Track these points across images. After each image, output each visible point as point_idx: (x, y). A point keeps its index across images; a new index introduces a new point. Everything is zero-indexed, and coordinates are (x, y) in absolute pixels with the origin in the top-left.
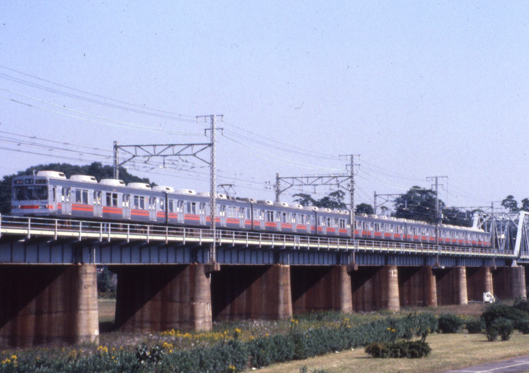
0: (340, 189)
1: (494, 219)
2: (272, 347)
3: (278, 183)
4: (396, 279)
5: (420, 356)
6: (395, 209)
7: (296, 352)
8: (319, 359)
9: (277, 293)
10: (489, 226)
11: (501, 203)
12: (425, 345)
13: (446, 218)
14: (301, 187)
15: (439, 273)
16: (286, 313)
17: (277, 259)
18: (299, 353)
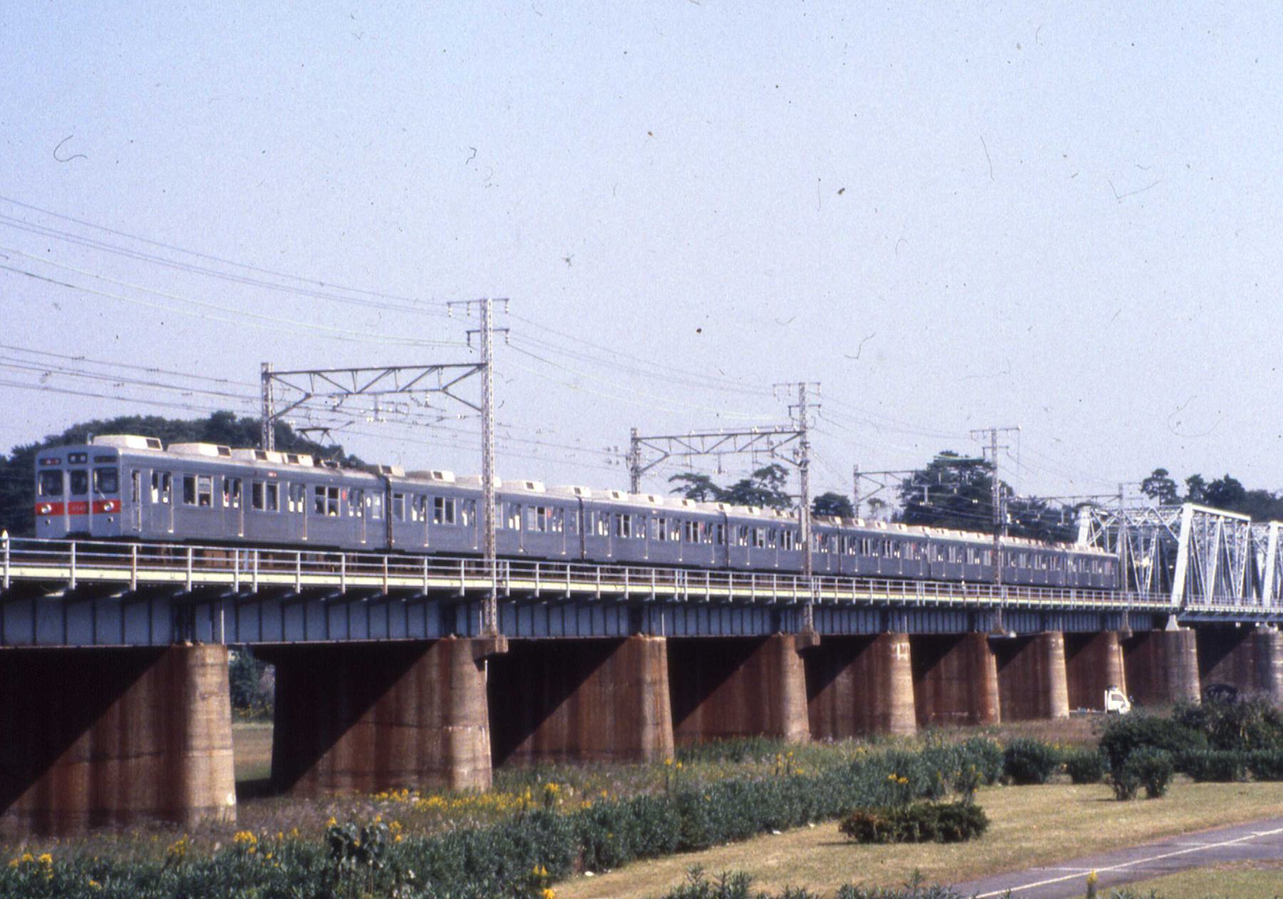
0: (778, 461)
1: (1125, 524)
2: (628, 824)
3: (635, 450)
4: (908, 665)
5: (965, 836)
6: (901, 506)
7: (684, 834)
8: (735, 849)
9: (639, 702)
10: (1113, 539)
11: (1140, 487)
12: (976, 811)
13: (1018, 522)
14: (688, 458)
15: (1005, 650)
16: (659, 749)
17: (636, 625)
18: (691, 836)
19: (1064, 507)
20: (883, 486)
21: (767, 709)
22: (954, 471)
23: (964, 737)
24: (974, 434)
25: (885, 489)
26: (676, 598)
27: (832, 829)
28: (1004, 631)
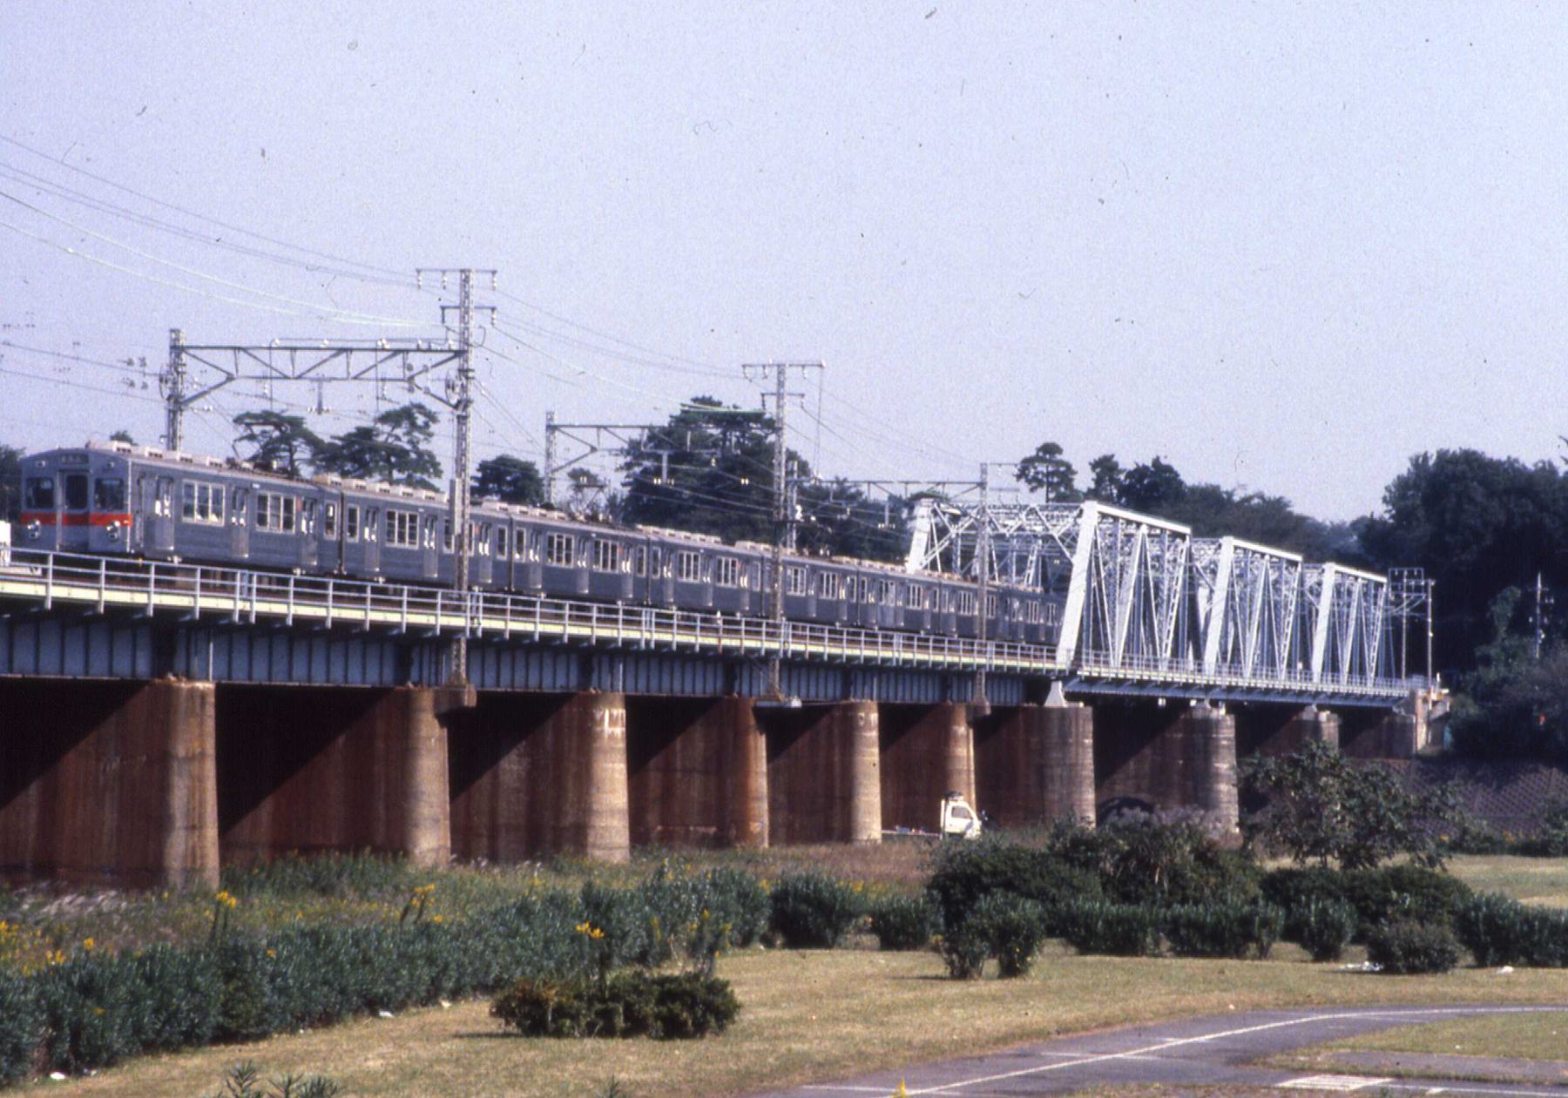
0: (419, 397)
1: (988, 530)
2: (132, 993)
3: (176, 367)
4: (621, 745)
5: (699, 1030)
6: (624, 485)
7: (226, 1014)
8: (315, 1040)
9: (164, 788)
10: (968, 555)
11: (1016, 471)
12: (718, 988)
13: (813, 518)
14: (267, 384)
15: (780, 727)
16: (193, 870)
17: (164, 660)
18: (238, 1016)
19: (892, 498)
20: (593, 449)
21: (381, 809)
22: (715, 431)
23: (706, 867)
24: (748, 370)
25: (598, 454)
26: (236, 618)
27: (478, 1011)
28: (781, 697)
